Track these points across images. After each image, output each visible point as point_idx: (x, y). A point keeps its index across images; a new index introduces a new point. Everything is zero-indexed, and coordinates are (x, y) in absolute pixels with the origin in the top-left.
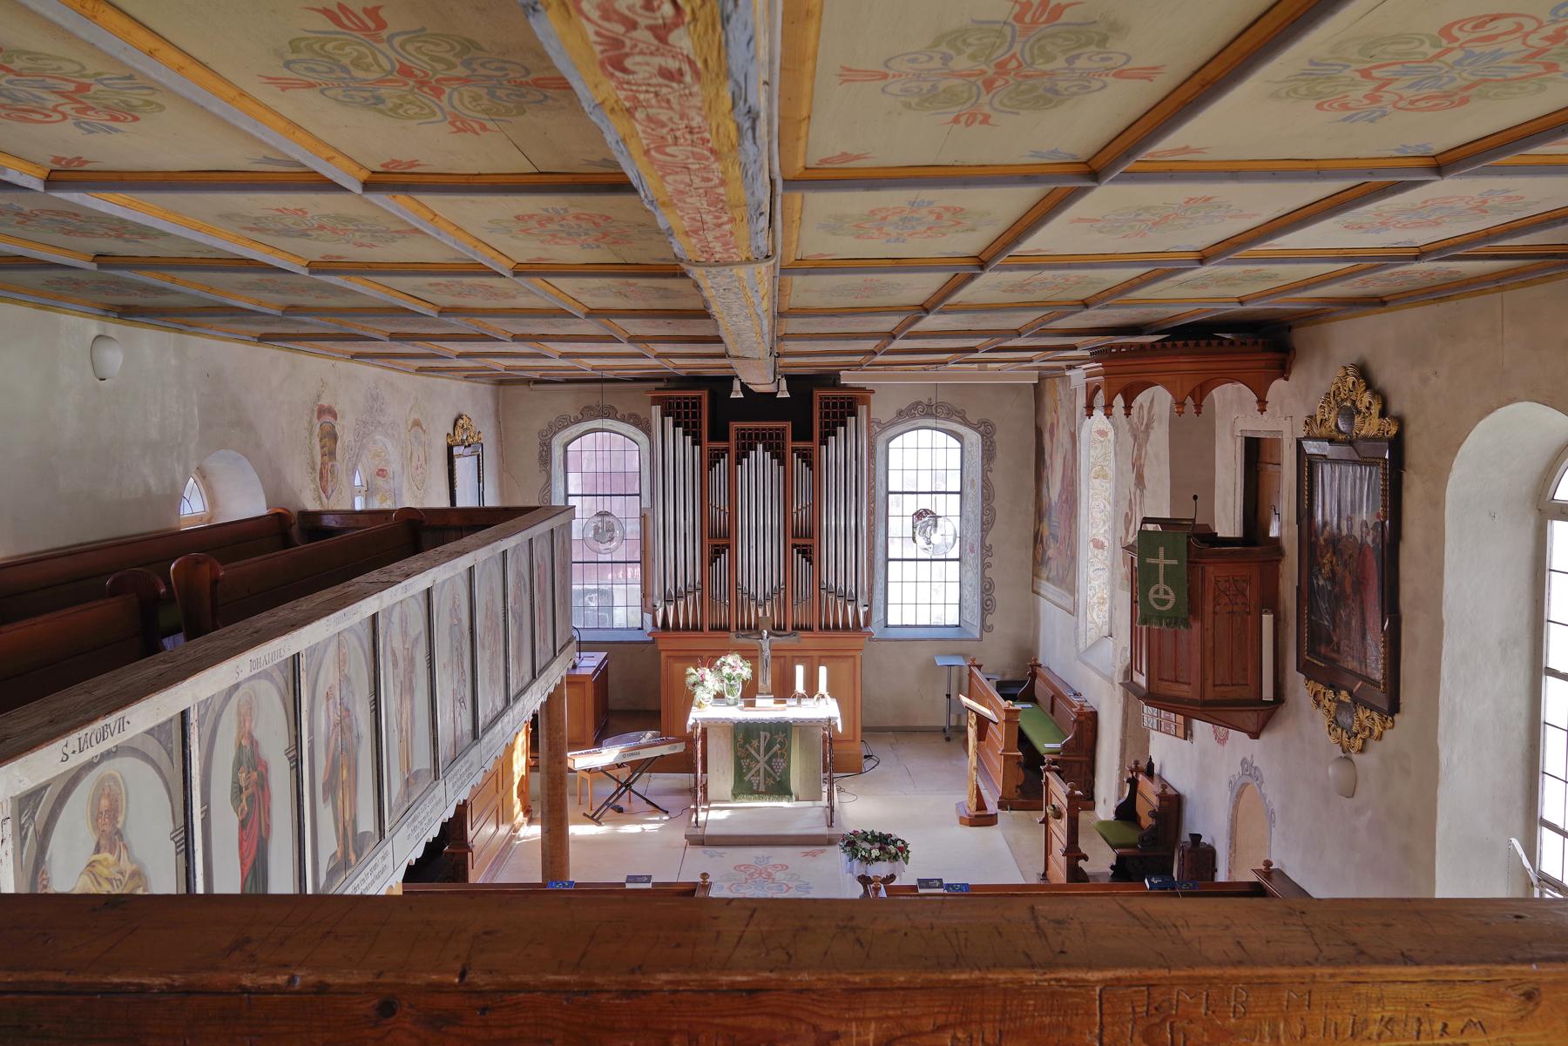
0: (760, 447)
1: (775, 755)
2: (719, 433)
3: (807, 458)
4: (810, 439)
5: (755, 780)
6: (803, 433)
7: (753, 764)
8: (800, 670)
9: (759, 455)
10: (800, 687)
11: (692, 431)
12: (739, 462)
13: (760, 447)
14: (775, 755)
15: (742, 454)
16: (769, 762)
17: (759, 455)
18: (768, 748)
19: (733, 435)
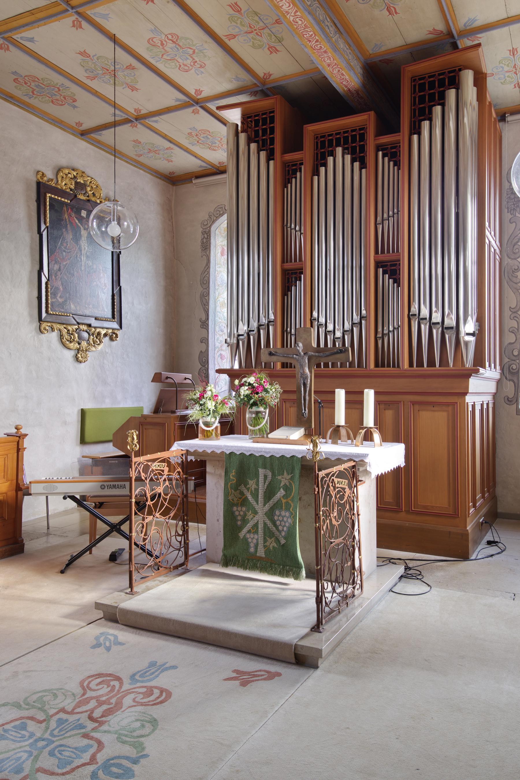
0: (339, 151)
1: (277, 505)
2: (294, 143)
3: (393, 154)
4: (395, 129)
5: (253, 539)
6: (388, 124)
7: (250, 515)
8: (341, 395)
9: (340, 160)
10: (340, 418)
11: (266, 145)
12: (316, 172)
13: (339, 151)
14: (277, 505)
15: (320, 161)
16: (270, 514)
17: (340, 160)
18: (269, 493)
19: (308, 143)
